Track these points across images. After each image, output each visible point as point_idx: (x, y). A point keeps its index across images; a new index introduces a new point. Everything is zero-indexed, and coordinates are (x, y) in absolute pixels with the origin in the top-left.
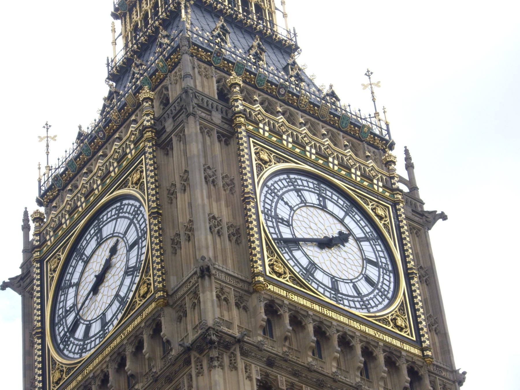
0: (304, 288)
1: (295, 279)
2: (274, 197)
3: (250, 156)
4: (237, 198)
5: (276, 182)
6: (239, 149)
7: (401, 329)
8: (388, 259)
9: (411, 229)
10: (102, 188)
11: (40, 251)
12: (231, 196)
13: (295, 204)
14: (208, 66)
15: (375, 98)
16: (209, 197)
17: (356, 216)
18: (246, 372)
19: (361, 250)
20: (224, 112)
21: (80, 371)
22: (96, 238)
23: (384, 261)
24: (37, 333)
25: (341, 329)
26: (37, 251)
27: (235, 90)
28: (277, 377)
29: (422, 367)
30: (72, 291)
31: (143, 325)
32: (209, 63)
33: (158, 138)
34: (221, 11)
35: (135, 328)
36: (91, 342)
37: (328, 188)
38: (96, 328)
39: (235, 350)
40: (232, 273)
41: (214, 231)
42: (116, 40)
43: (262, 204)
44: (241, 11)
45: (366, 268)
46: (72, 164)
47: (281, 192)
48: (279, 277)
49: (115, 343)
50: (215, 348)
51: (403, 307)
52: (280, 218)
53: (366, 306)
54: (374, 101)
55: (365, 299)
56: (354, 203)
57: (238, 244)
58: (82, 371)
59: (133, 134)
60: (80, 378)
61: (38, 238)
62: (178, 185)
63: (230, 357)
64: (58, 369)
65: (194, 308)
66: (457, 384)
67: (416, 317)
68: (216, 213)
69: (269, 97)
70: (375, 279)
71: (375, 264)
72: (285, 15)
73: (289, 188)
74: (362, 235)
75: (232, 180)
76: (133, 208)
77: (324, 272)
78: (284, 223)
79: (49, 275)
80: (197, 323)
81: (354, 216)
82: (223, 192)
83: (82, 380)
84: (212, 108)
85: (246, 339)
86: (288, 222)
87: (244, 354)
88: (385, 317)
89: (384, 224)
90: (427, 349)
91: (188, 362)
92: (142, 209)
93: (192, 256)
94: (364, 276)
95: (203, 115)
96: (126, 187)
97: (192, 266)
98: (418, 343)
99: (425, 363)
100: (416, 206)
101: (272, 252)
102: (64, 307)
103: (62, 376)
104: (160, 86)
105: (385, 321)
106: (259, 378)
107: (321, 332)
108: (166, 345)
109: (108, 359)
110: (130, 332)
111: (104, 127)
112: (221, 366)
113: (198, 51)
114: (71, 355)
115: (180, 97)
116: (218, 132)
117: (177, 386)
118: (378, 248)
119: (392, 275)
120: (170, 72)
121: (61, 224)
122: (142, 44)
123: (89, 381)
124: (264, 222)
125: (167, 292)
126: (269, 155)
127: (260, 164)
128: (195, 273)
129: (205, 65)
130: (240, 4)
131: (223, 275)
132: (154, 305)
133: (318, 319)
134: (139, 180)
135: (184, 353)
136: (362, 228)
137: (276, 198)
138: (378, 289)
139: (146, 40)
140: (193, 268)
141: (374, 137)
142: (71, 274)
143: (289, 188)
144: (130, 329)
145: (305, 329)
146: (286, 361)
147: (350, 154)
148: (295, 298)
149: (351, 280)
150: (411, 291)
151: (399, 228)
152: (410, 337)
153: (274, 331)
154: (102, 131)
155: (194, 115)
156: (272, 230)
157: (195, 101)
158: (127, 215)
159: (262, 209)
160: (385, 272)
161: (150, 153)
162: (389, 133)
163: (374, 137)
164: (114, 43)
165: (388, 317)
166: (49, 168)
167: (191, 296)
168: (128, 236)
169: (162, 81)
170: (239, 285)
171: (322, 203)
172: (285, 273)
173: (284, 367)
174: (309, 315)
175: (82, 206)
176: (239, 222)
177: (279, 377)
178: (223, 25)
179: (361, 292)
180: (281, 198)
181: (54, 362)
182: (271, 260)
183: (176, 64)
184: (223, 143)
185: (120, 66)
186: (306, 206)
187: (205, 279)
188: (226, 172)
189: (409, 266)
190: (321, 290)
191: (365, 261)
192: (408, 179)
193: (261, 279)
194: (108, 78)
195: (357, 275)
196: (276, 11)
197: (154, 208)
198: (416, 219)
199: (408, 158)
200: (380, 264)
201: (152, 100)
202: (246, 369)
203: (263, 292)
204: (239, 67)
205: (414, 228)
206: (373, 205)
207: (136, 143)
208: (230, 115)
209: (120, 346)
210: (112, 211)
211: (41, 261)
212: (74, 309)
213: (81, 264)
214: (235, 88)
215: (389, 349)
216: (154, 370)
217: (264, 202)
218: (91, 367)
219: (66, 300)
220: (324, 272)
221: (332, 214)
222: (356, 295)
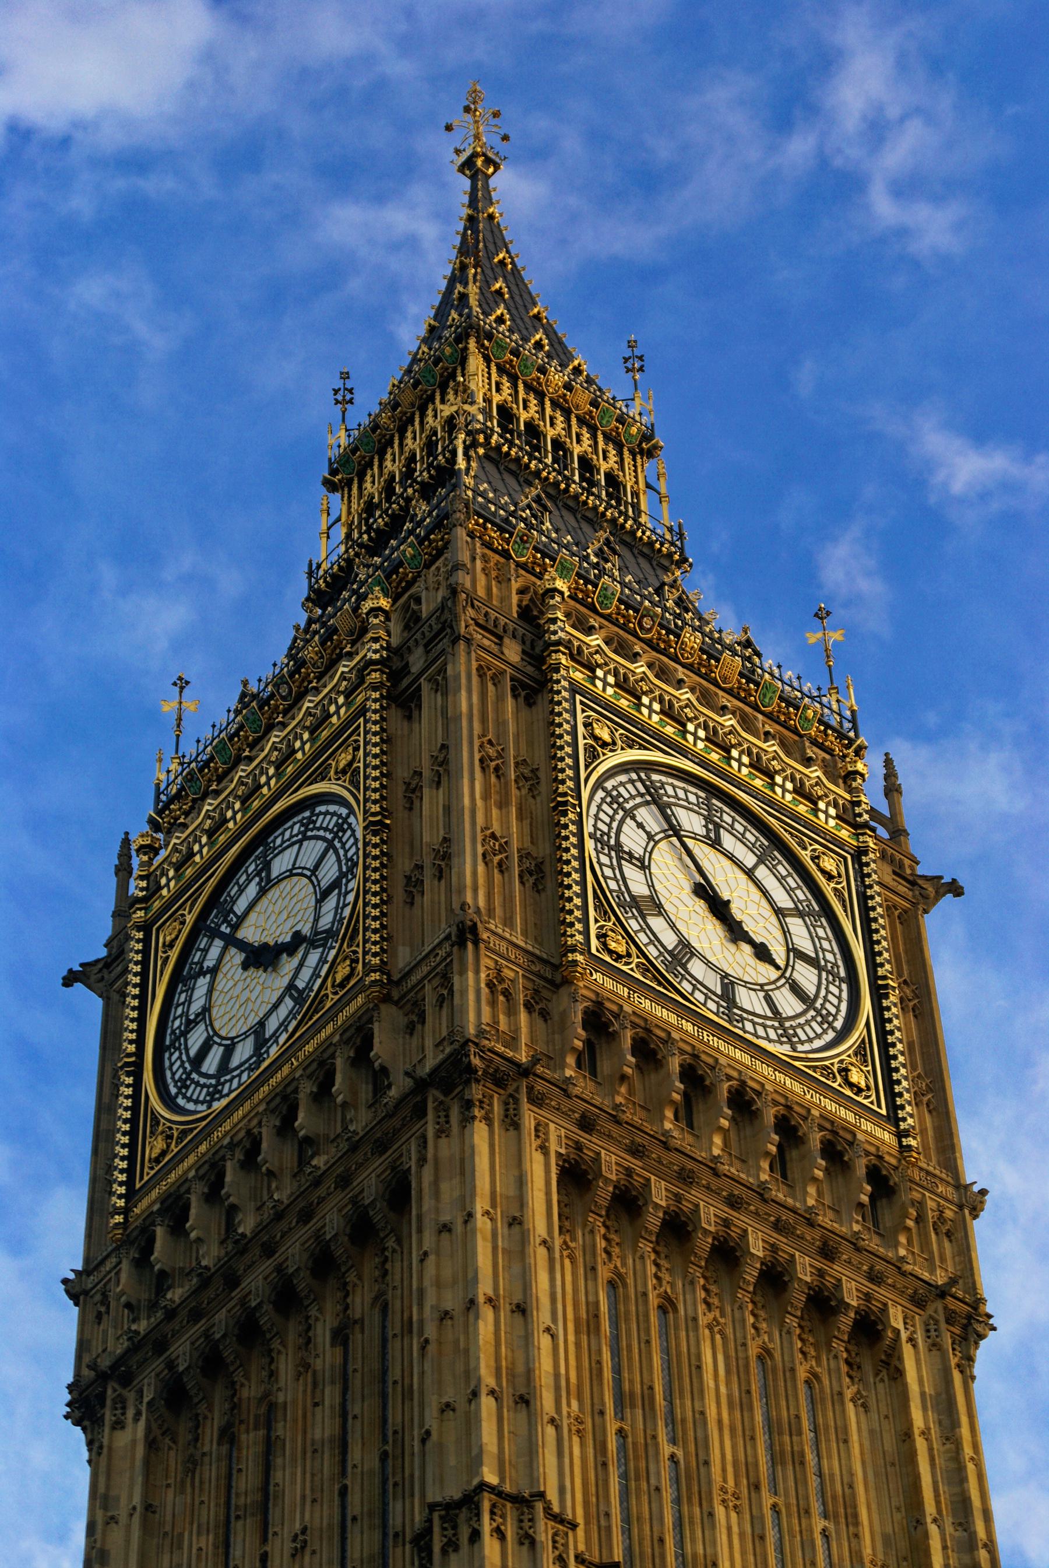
0: (665, 988)
1: (648, 967)
2: (616, 812)
3: (575, 727)
4: (540, 807)
6: (552, 712)
8: (838, 956)
9: (888, 908)
11: (145, 909)
12: (531, 800)
14: (502, 560)
17: (780, 868)
18: (537, 1136)
19: (786, 932)
20: (528, 643)
21: (205, 1134)
22: (257, 879)
23: (832, 956)
24: (127, 1064)
25: (735, 1074)
26: (140, 909)
27: (552, 602)
28: (599, 1154)
30: (203, 982)
31: (337, 1038)
32: (505, 554)
33: (394, 685)
34: (537, 473)
35: (319, 1046)
36: (231, 1081)
37: (725, 809)
38: (243, 1051)
39: (517, 1090)
40: (522, 944)
41: (492, 861)
43: (591, 821)
44: (576, 478)
46: (224, 749)
47: (631, 803)
48: (615, 960)
50: (478, 1081)
51: (865, 1049)
53: (788, 1037)
55: (787, 1024)
57: (538, 891)
59: (345, 679)
60: (203, 1148)
61: (144, 884)
62: (426, 773)
63: (506, 1104)
64: (163, 1132)
65: (441, 1007)
66: (967, 1212)
67: (888, 1071)
68: (496, 827)
69: (621, 632)
70: (811, 989)
71: (813, 962)
74: (792, 906)
75: (534, 771)
76: (335, 818)
77: (708, 963)
79: (160, 954)
80: (444, 1033)
81: (774, 866)
82: (514, 791)
83: (208, 1150)
84: (505, 631)
85: (539, 1069)
86: (641, 860)
88: (826, 1063)
89: (835, 889)
90: (906, 1134)
91: (420, 1112)
92: (352, 819)
93: (443, 906)
95: (486, 642)
96: (323, 779)
97: (443, 926)
98: (893, 1118)
100: (901, 865)
101: (606, 913)
103: (168, 1146)
104: (406, 595)
105: (827, 1070)
106: (563, 1151)
107: (696, 1078)
108: (380, 1078)
109: (261, 1108)
110: (311, 1054)
111: (291, 675)
113: (486, 529)
114: (191, 1106)
115: (442, 607)
116: (512, 679)
117: (394, 1161)
118: (821, 932)
119: (844, 986)
120: (427, 566)
121: (191, 854)
122: (378, 531)
123: (221, 1153)
124: (593, 854)
125: (389, 975)
127: (592, 746)
128: (448, 937)
129: (497, 557)
130: (576, 465)
131: (504, 944)
134: (350, 764)
135: (413, 1092)
136: (789, 891)
137: (621, 813)
138: (815, 1009)
139: (386, 524)
140: (444, 929)
142: (202, 950)
144: (309, 1048)
145: (662, 1066)
146: (617, 1122)
147: (775, 748)
149: (762, 985)
150: (881, 1021)
152: (875, 1108)
153: (598, 1064)
154: (287, 683)
156: (608, 872)
157: (471, 612)
158: (321, 833)
159: (591, 830)
160: (831, 978)
161: (375, 712)
163: (825, 731)
167: (436, 982)
168: (321, 874)
169: (410, 584)
171: (712, 835)
172: (629, 955)
175: (235, 819)
176: (543, 850)
178: (538, 496)
180: (630, 814)
181: (156, 1120)
182: (601, 927)
183: (440, 552)
184: (521, 700)
185: (333, 576)
187: (465, 947)
188: (524, 754)
189: (881, 972)
190: (701, 997)
193: (580, 958)
197: (374, 814)
198: (902, 889)
199: (890, 774)
200: (823, 963)
202: (537, 1130)
203: (581, 984)
207: (348, 694)
208: (538, 650)
209: (290, 1081)
211: (146, 927)
212: (204, 1018)
214: (553, 598)
215: (832, 1127)
216: (352, 1128)
217: (597, 818)
218: (227, 1126)
219: (189, 1001)
220: (708, 963)
221: (731, 857)
222: (770, 1014)
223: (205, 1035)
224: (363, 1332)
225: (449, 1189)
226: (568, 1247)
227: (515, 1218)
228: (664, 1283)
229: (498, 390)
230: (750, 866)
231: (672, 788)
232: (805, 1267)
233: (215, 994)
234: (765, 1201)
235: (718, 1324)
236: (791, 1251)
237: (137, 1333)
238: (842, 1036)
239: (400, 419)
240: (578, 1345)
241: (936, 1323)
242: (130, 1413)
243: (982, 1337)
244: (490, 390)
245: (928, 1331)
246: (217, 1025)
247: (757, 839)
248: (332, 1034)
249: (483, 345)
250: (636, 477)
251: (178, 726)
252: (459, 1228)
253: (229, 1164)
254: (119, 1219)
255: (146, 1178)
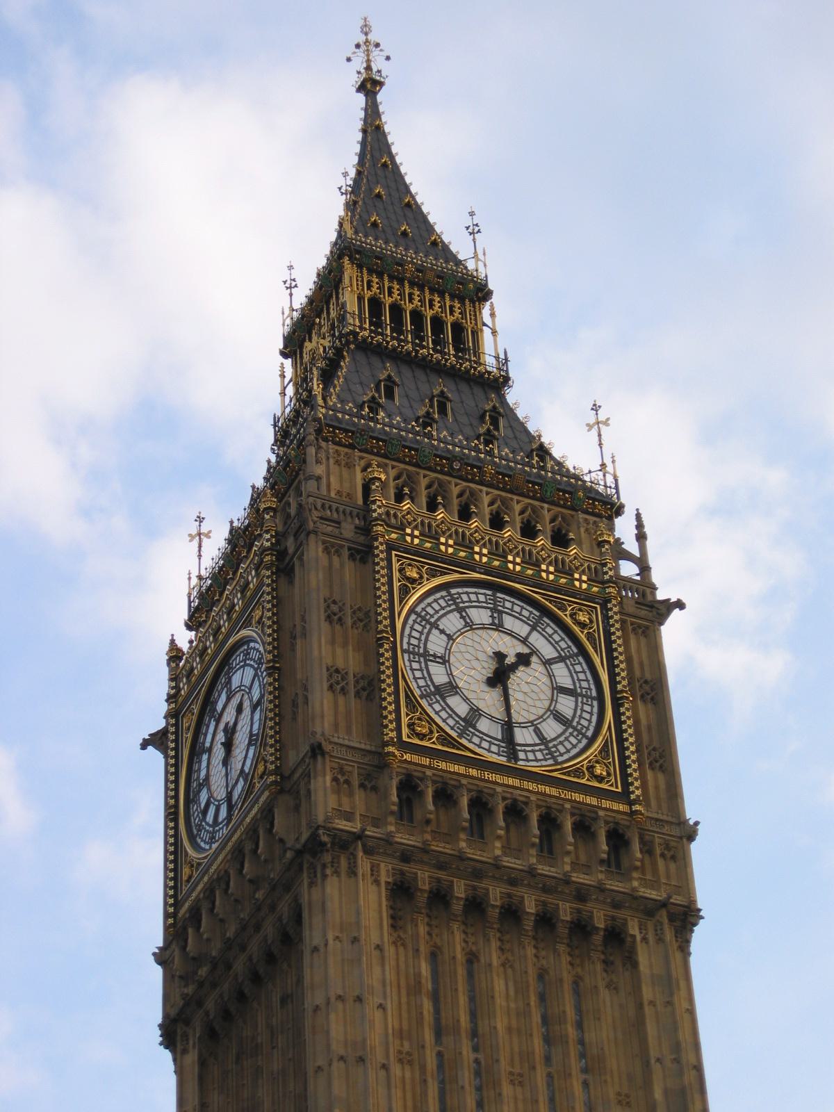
1: (446, 739)
2: (424, 627)
5: (429, 605)
7: (600, 779)
8: (591, 682)
10: (229, 624)
13: (455, 630)
15: (603, 442)
16: (333, 642)
18: (372, 875)
19: (551, 676)
20: (361, 517)
23: (587, 685)
25: (509, 795)
27: (374, 487)
29: (628, 827)
30: (205, 757)
31: (259, 816)
32: (352, 446)
35: (252, 819)
39: (355, 849)
42: (285, 388)
45: (556, 701)
48: (422, 740)
49: (234, 839)
50: (328, 851)
52: (431, 655)
54: (601, 448)
55: (551, 745)
56: (545, 612)
58: (207, 870)
60: (206, 879)
63: (349, 859)
64: (190, 863)
66: (685, 840)
68: (340, 664)
72: (494, 332)
73: (448, 609)
74: (555, 655)
78: (438, 660)
87: (368, 852)
91: (301, 869)
94: (552, 713)
99: (633, 822)
100: (644, 595)
101: (414, 706)
102: (198, 777)
105: (578, 772)
106: (390, 880)
112: (337, 873)
114: (202, 844)
116: (350, 549)
118: (578, 668)
119: (595, 703)
124: (407, 663)
126: (420, 569)
128: (308, 752)
129: (346, 450)
131: (344, 749)
132: (267, 793)
133: (475, 788)
134: (261, 618)
136: (554, 645)
137: (428, 626)
140: (305, 749)
141: (593, 503)
143: (448, 609)
148: (443, 765)
149: (532, 722)
151: (608, 634)
155: (316, 533)
156: (418, 674)
157: (315, 514)
158: (252, 663)
159: (405, 646)
162: (617, 492)
164: (283, 394)
165: (582, 766)
166: (200, 578)
168: (253, 691)
170: (366, 760)
171: (496, 621)
172: (431, 732)
173: (425, 860)
174: (461, 785)
177: (419, 874)
179: (546, 736)
180: (435, 625)
181: (186, 851)
184: (357, 562)
186: (472, 629)
190: (485, 745)
191: (555, 691)
192: (638, 555)
194: (273, 445)
195: (541, 712)
196: (484, 328)
199: (640, 526)
200: (579, 691)
201: (274, 510)
202: (372, 870)
204: (393, 445)
205: (640, 626)
206: (573, 609)
210: (238, 658)
213: (213, 723)
217: (410, 636)
219: (199, 770)
221: (510, 634)
222: (538, 741)
223: (207, 796)
224: (292, 1002)
225: (317, 920)
226: (401, 939)
227: (355, 938)
228: (470, 944)
229: (369, 287)
230: (524, 634)
231: (466, 595)
232: (566, 911)
233: (211, 767)
234: (534, 876)
235: (509, 961)
236: (556, 902)
237: (187, 995)
238: (591, 741)
239: (316, 310)
240: (408, 1003)
241: (661, 924)
242: (191, 1042)
243: (695, 924)
244: (363, 290)
245: (656, 930)
246: (213, 788)
247: (531, 613)
248: (256, 814)
249: (356, 259)
250: (476, 320)
251: (200, 551)
252: (322, 949)
253: (217, 893)
254: (171, 921)
255: (184, 892)
